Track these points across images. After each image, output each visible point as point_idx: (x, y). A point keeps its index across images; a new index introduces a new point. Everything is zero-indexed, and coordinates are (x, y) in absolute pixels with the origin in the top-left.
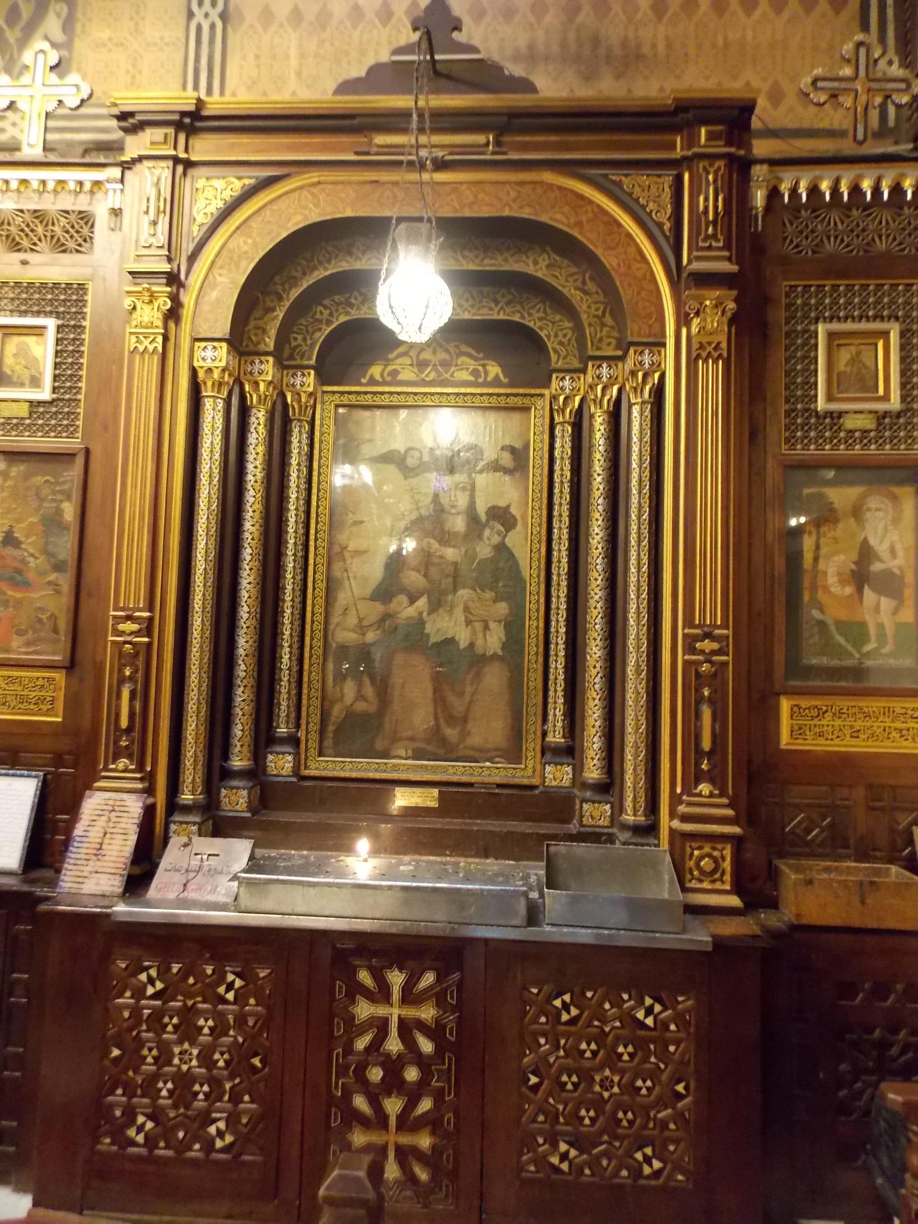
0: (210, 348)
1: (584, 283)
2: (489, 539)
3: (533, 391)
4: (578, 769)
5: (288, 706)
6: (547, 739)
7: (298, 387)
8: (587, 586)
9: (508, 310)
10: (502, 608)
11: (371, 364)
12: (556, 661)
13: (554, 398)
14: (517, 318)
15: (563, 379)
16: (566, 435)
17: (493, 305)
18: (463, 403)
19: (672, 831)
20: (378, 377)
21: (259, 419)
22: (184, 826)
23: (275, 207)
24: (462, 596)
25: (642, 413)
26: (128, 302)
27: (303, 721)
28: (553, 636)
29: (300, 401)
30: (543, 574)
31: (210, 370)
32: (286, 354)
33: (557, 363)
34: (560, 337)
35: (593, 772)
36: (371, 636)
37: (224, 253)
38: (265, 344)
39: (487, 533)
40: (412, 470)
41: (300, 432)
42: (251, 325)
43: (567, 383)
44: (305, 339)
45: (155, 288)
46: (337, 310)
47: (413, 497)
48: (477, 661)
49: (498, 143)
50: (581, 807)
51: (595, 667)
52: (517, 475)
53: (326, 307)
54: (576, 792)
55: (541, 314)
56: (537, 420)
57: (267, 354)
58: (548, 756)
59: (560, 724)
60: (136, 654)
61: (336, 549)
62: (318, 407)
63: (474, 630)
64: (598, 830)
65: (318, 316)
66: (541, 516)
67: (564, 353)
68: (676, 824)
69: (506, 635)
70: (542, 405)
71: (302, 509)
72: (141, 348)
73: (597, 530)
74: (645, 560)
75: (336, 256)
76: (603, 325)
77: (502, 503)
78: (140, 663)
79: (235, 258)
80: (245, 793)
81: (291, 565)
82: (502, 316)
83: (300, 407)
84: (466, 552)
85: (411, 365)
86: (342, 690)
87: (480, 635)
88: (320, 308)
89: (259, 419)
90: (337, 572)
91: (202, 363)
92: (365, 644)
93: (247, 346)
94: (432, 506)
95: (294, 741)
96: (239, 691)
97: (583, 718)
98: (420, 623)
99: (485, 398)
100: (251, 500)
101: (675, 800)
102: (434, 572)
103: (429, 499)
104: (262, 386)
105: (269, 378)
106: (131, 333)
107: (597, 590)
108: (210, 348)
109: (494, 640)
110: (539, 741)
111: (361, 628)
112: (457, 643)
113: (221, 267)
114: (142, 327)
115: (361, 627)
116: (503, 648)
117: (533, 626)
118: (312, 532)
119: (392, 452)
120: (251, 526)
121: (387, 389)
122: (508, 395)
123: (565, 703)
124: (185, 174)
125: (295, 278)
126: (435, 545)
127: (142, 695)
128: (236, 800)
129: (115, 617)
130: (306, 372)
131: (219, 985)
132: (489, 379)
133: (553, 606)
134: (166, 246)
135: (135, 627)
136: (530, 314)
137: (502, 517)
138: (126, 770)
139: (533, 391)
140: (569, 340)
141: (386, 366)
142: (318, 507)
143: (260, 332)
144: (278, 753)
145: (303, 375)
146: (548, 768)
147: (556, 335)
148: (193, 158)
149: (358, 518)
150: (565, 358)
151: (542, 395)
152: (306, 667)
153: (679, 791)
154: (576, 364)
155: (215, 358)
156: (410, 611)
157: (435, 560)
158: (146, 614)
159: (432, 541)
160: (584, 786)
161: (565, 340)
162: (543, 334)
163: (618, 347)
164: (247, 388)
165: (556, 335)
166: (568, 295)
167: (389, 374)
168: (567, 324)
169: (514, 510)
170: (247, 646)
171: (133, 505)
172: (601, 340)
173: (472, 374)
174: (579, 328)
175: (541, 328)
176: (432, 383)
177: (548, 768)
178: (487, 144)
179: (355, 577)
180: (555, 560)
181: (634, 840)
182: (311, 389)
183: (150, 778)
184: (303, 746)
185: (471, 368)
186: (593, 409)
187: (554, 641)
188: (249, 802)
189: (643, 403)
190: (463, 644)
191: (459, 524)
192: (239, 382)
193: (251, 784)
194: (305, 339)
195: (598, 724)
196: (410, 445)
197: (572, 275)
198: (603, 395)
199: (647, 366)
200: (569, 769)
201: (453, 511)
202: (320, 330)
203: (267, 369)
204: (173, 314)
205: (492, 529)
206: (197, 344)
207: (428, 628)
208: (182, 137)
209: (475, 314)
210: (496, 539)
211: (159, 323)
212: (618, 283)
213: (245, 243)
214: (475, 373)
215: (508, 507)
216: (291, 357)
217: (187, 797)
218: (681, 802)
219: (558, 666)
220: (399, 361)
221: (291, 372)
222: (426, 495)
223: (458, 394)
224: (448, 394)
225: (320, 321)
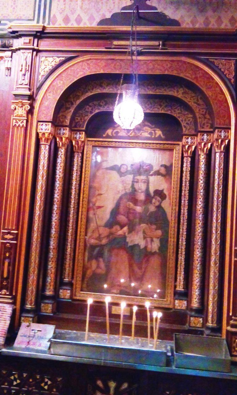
0: (44, 125)
1: (198, 100)
2: (154, 203)
3: (175, 143)
4: (189, 302)
5: (69, 270)
6: (177, 289)
7: (78, 139)
8: (195, 226)
9: (166, 109)
10: (159, 232)
11: (108, 129)
12: (181, 256)
13: (183, 146)
14: (169, 113)
15: (188, 138)
16: (189, 162)
17: (159, 107)
18: (145, 146)
19: (227, 331)
20: (110, 134)
21: (62, 152)
22: (27, 318)
23: (72, 69)
25: (220, 156)
26: (13, 107)
27: (75, 276)
28: (180, 245)
29: (78, 144)
30: (177, 219)
31: (44, 134)
32: (73, 125)
33: (185, 132)
34: (187, 121)
35: (195, 303)
36: (104, 241)
37: (51, 87)
38: (66, 122)
39: (154, 201)
40: (123, 173)
41: (78, 157)
42: (60, 114)
43: (189, 140)
44: (81, 119)
45: (24, 101)
46: (95, 108)
47: (123, 185)
48: (147, 254)
49: (164, 45)
50: (190, 319)
51: (197, 260)
52: (167, 177)
53: (90, 106)
54: (189, 312)
55: (179, 111)
56: (177, 151)
57: (66, 126)
58: (177, 296)
59: (182, 283)
61: (91, 205)
62: (86, 147)
64: (197, 329)
65: (87, 110)
66: (176, 195)
68: (229, 328)
70: (178, 149)
71: (77, 188)
72: (17, 125)
73: (200, 203)
74: (220, 217)
75: (96, 87)
76: (205, 118)
77: (160, 189)
78: (12, 251)
79: (55, 89)
80: (51, 305)
81: (72, 212)
82: (163, 112)
83: (78, 147)
84: (145, 208)
86: (91, 265)
87: (149, 243)
88: (88, 106)
89: (62, 152)
90: (91, 215)
91: (41, 131)
93: (58, 123)
94: (131, 189)
95: (70, 284)
96: (50, 263)
97: (192, 281)
98: (125, 237)
99: (155, 145)
100: (58, 185)
101: (229, 318)
102: (131, 215)
103: (130, 186)
104: (64, 139)
105: (67, 136)
106: (13, 119)
107: (199, 228)
109: (155, 246)
110: (173, 290)
111: (99, 238)
113: (50, 93)
114: (18, 117)
117: (172, 240)
118: (81, 198)
119: (116, 166)
120: (57, 196)
121: (114, 140)
122: (164, 144)
123: (184, 274)
124: (36, 55)
125: (79, 96)
126: (132, 205)
127: (12, 264)
128: (48, 308)
129: (3, 232)
130: (81, 132)
131: (42, 383)
133: (181, 233)
134: (28, 84)
135: (11, 237)
136: (175, 111)
137: (160, 194)
138: (5, 295)
139: (175, 143)
140: (191, 122)
141: (114, 130)
142: (84, 188)
143: (64, 117)
144: (64, 289)
145: (80, 134)
146: (176, 301)
147: (185, 120)
148: (40, 49)
149: (100, 192)
150: (189, 130)
151: (179, 145)
152: (77, 254)
153: (231, 314)
154: (193, 132)
155: (46, 129)
156: (120, 232)
157: (131, 211)
158: (16, 232)
159: (131, 203)
160: (192, 310)
161: (189, 122)
162: (180, 119)
163: (211, 128)
164: (58, 140)
165: (185, 120)
166: (191, 105)
167: (115, 133)
168: (190, 116)
169: (166, 192)
170: (54, 245)
171: (12, 187)
172: (204, 124)
174: (195, 118)
175: (179, 117)
177: (176, 301)
178: (159, 45)
179: (98, 217)
180: (182, 213)
181: (211, 334)
182: (83, 140)
183: (14, 298)
184: (74, 287)
185: (149, 131)
186: (200, 153)
187: (180, 248)
188: (53, 309)
189: (221, 152)
190: (142, 246)
191: (142, 197)
192: (55, 138)
193: (53, 302)
194: (81, 119)
195: (198, 284)
196: (122, 163)
197: (192, 97)
198: (204, 146)
199: (223, 137)
200: (185, 302)
202: (87, 115)
203: (66, 132)
204: (30, 112)
205: (156, 199)
206: (39, 123)
207: (128, 240)
208: (36, 40)
209: (151, 111)
210: (157, 204)
211: (25, 115)
212: (211, 103)
213: (60, 83)
214: (151, 133)
215: (162, 191)
216: (76, 126)
217: (28, 306)
218: (232, 319)
219: (182, 258)
221: (75, 132)
222: (129, 184)
223: (143, 143)
224: (139, 143)
225: (87, 112)
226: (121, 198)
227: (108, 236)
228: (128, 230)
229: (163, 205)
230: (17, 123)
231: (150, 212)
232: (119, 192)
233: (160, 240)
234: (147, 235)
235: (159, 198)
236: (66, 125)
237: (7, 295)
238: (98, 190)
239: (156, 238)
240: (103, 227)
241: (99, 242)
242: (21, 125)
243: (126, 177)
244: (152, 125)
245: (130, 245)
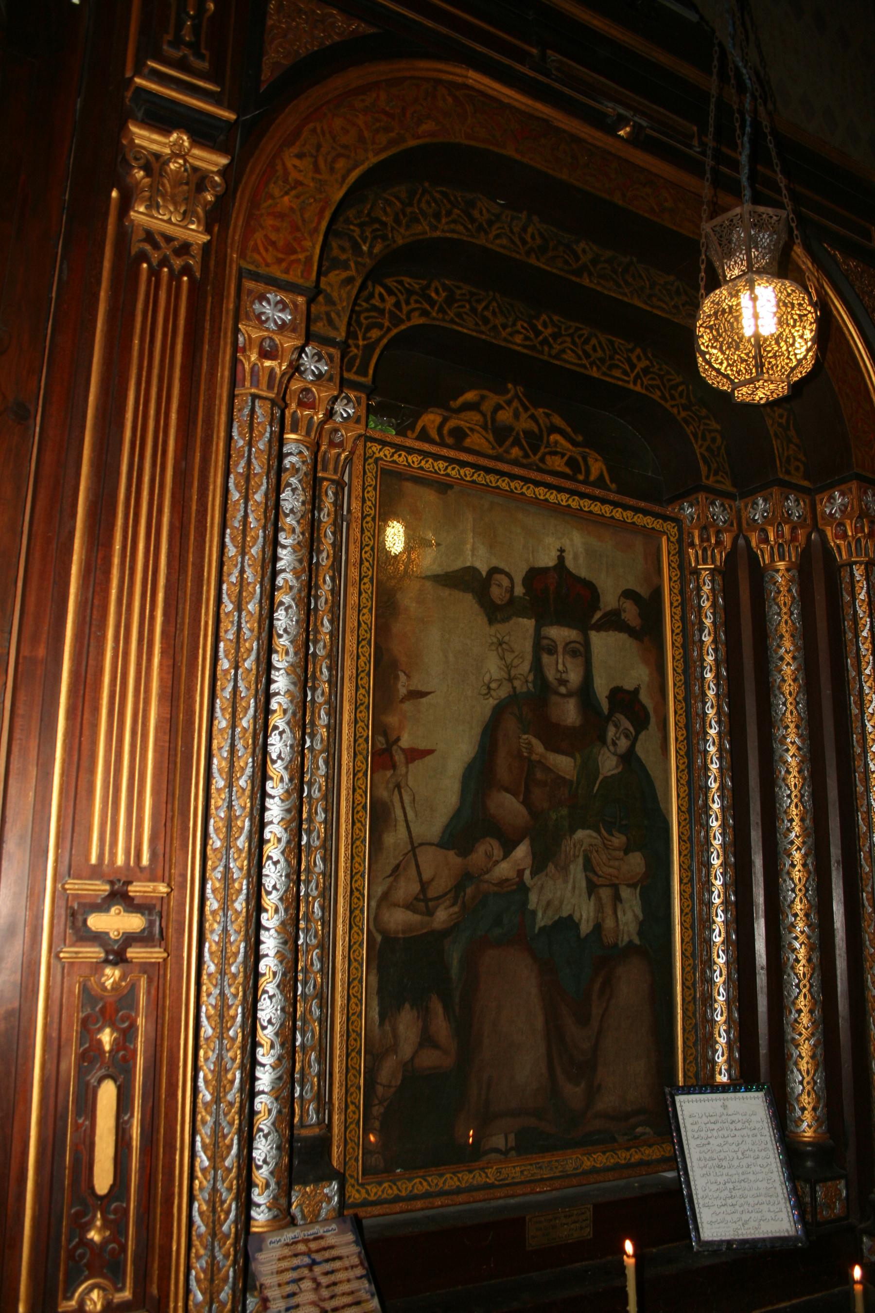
10: (636, 862)
24: (581, 842)
36: (442, 916)
39: (611, 732)
47: (502, 658)
63: (599, 899)
67: (714, 466)
69: (644, 910)
85: (485, 428)
87: (609, 911)
92: (432, 932)
94: (531, 678)
109: (628, 918)
112: (577, 926)
115: (426, 900)
116: (640, 933)
119: (472, 570)
126: (539, 747)
132: (592, 478)
149: (417, 684)
156: (504, 869)
159: (535, 741)
169: (644, 697)
173: (567, 464)
176: (515, 463)
185: (569, 454)
190: (585, 928)
196: (495, 562)
201: (563, 690)
210: (623, 744)
214: (572, 463)
215: (637, 691)
220: (463, 415)
226: (499, 712)
227: (459, 888)
228: (529, 861)
229: (639, 750)
231: (601, 777)
232: (489, 688)
233: (641, 894)
234: (596, 874)
235: (626, 724)
238: (408, 676)
239: (628, 886)
240: (437, 845)
241: (427, 918)
243: (512, 622)
245: (542, 924)
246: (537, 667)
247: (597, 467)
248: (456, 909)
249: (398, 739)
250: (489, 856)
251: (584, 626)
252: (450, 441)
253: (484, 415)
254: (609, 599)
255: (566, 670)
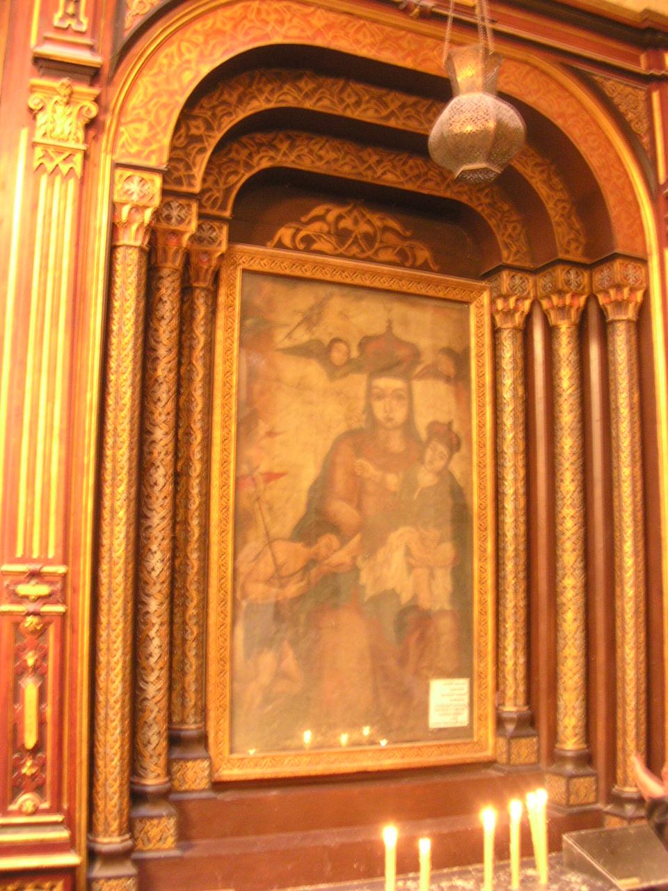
20: (287, 241)
33: (508, 258)
39: (429, 454)
60: (42, 633)
72: (50, 167)
91: (124, 199)
94: (364, 417)
108: (136, 179)
135: (44, 590)
138: (36, 811)
140: (519, 235)
141: (298, 230)
158: (61, 569)
191: (396, 443)
194: (216, 182)
201: (389, 425)
202: (236, 173)
206: (119, 172)
210: (439, 464)
214: (402, 253)
215: (450, 424)
227: (306, 569)
230: (52, 159)
231: (419, 489)
236: (191, 190)
237: (46, 812)
242: (65, 168)
244: (407, 229)
246: (369, 410)
247: (424, 254)
248: (302, 584)
249: (258, 467)
250: (329, 547)
251: (407, 376)
252: (302, 246)
253: (329, 224)
254: (428, 358)
255: (390, 411)
